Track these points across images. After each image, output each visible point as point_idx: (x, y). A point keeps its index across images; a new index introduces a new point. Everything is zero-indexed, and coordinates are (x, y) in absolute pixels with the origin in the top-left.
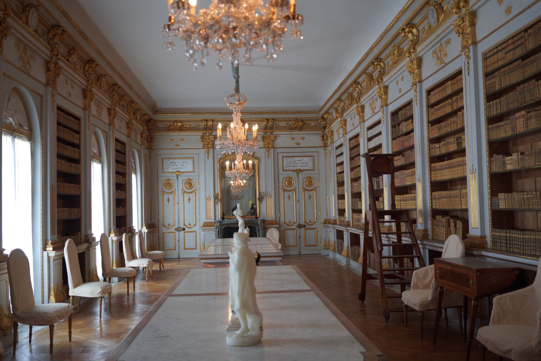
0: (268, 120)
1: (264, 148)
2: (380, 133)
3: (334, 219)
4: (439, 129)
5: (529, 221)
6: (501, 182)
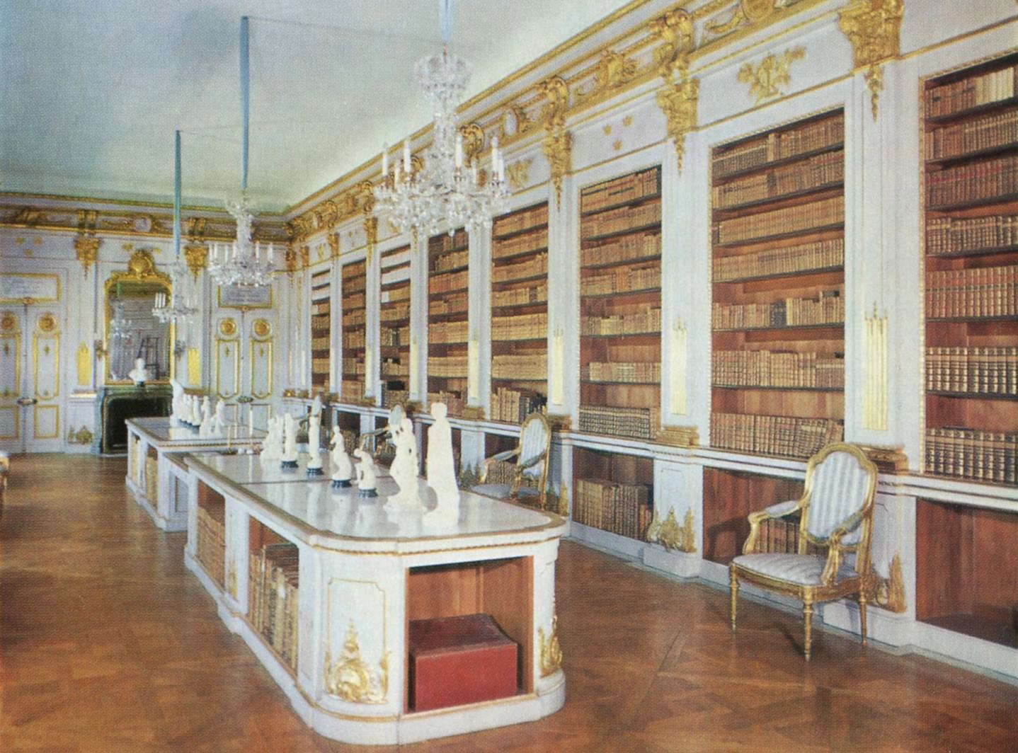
0: (197, 219)
2: (407, 264)
3: (303, 388)
4: (509, 272)
5: (623, 394)
6: (594, 349)
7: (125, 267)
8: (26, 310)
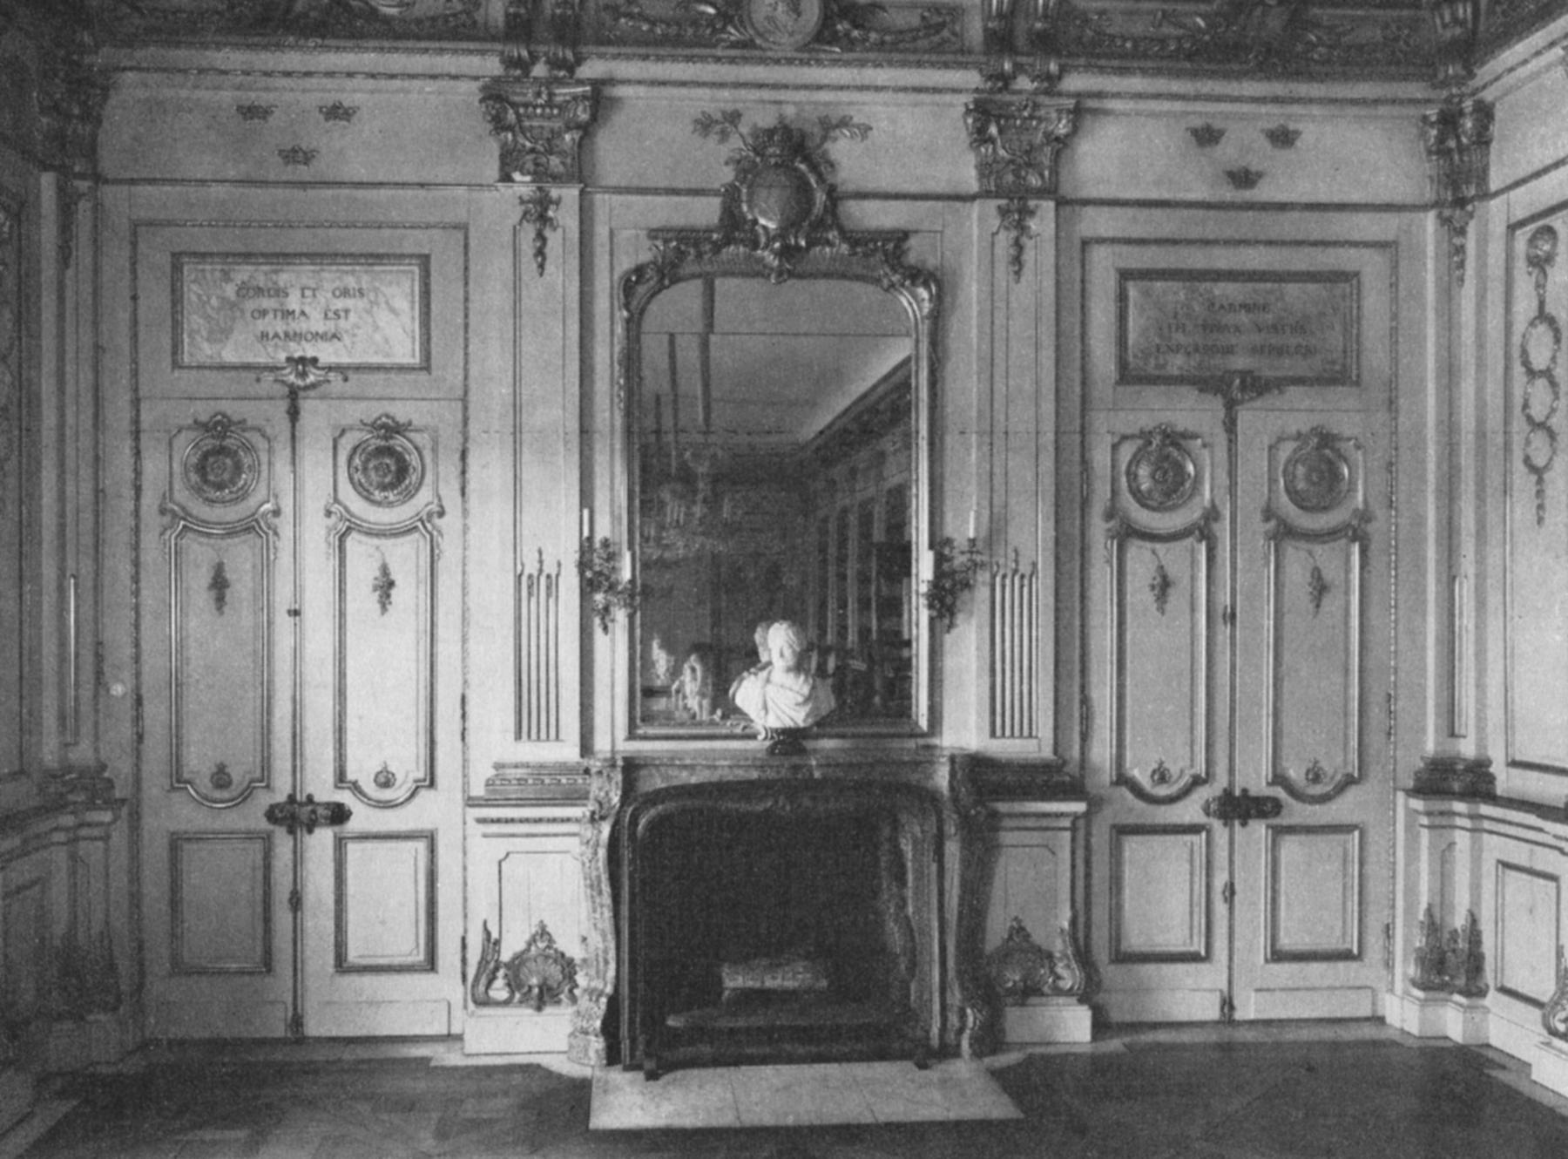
1: (985, 194)
7: (706, 212)
8: (294, 414)
